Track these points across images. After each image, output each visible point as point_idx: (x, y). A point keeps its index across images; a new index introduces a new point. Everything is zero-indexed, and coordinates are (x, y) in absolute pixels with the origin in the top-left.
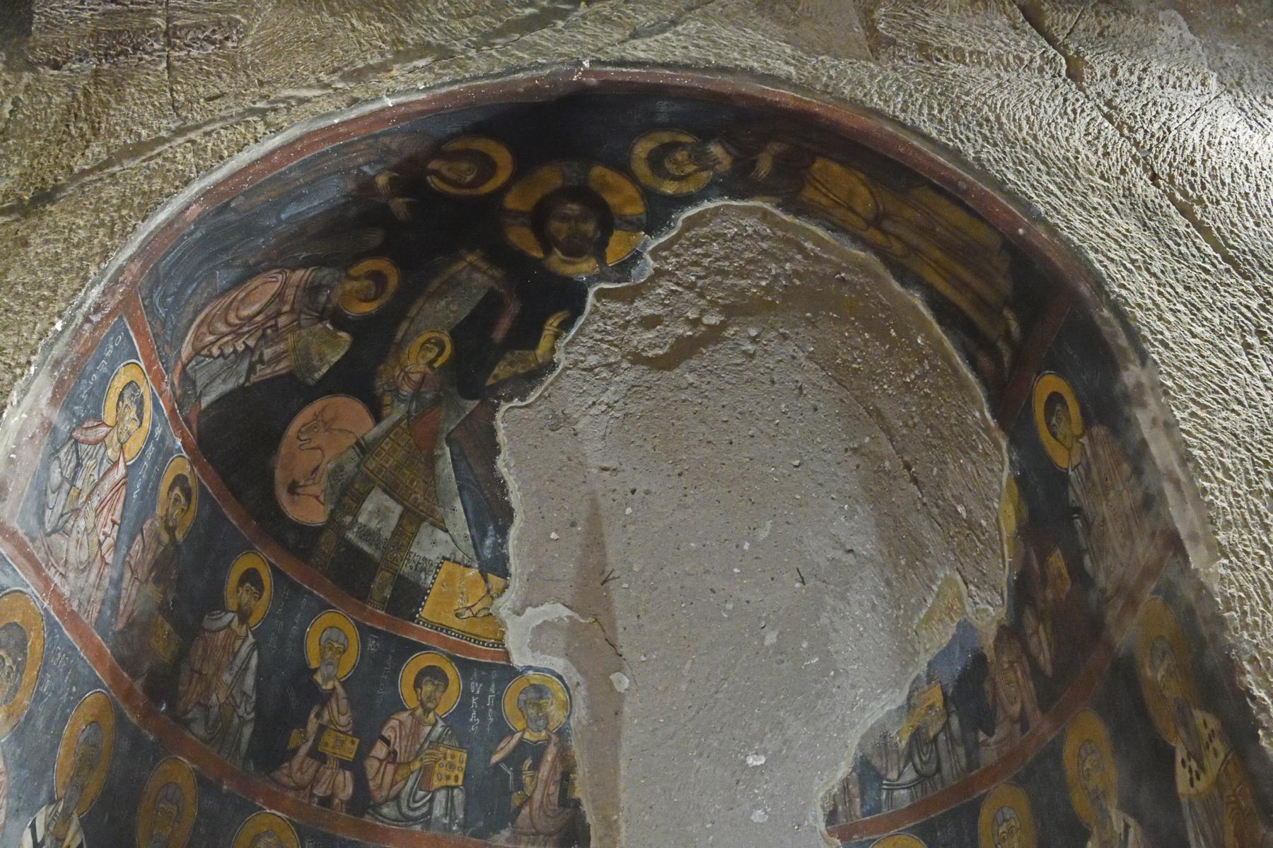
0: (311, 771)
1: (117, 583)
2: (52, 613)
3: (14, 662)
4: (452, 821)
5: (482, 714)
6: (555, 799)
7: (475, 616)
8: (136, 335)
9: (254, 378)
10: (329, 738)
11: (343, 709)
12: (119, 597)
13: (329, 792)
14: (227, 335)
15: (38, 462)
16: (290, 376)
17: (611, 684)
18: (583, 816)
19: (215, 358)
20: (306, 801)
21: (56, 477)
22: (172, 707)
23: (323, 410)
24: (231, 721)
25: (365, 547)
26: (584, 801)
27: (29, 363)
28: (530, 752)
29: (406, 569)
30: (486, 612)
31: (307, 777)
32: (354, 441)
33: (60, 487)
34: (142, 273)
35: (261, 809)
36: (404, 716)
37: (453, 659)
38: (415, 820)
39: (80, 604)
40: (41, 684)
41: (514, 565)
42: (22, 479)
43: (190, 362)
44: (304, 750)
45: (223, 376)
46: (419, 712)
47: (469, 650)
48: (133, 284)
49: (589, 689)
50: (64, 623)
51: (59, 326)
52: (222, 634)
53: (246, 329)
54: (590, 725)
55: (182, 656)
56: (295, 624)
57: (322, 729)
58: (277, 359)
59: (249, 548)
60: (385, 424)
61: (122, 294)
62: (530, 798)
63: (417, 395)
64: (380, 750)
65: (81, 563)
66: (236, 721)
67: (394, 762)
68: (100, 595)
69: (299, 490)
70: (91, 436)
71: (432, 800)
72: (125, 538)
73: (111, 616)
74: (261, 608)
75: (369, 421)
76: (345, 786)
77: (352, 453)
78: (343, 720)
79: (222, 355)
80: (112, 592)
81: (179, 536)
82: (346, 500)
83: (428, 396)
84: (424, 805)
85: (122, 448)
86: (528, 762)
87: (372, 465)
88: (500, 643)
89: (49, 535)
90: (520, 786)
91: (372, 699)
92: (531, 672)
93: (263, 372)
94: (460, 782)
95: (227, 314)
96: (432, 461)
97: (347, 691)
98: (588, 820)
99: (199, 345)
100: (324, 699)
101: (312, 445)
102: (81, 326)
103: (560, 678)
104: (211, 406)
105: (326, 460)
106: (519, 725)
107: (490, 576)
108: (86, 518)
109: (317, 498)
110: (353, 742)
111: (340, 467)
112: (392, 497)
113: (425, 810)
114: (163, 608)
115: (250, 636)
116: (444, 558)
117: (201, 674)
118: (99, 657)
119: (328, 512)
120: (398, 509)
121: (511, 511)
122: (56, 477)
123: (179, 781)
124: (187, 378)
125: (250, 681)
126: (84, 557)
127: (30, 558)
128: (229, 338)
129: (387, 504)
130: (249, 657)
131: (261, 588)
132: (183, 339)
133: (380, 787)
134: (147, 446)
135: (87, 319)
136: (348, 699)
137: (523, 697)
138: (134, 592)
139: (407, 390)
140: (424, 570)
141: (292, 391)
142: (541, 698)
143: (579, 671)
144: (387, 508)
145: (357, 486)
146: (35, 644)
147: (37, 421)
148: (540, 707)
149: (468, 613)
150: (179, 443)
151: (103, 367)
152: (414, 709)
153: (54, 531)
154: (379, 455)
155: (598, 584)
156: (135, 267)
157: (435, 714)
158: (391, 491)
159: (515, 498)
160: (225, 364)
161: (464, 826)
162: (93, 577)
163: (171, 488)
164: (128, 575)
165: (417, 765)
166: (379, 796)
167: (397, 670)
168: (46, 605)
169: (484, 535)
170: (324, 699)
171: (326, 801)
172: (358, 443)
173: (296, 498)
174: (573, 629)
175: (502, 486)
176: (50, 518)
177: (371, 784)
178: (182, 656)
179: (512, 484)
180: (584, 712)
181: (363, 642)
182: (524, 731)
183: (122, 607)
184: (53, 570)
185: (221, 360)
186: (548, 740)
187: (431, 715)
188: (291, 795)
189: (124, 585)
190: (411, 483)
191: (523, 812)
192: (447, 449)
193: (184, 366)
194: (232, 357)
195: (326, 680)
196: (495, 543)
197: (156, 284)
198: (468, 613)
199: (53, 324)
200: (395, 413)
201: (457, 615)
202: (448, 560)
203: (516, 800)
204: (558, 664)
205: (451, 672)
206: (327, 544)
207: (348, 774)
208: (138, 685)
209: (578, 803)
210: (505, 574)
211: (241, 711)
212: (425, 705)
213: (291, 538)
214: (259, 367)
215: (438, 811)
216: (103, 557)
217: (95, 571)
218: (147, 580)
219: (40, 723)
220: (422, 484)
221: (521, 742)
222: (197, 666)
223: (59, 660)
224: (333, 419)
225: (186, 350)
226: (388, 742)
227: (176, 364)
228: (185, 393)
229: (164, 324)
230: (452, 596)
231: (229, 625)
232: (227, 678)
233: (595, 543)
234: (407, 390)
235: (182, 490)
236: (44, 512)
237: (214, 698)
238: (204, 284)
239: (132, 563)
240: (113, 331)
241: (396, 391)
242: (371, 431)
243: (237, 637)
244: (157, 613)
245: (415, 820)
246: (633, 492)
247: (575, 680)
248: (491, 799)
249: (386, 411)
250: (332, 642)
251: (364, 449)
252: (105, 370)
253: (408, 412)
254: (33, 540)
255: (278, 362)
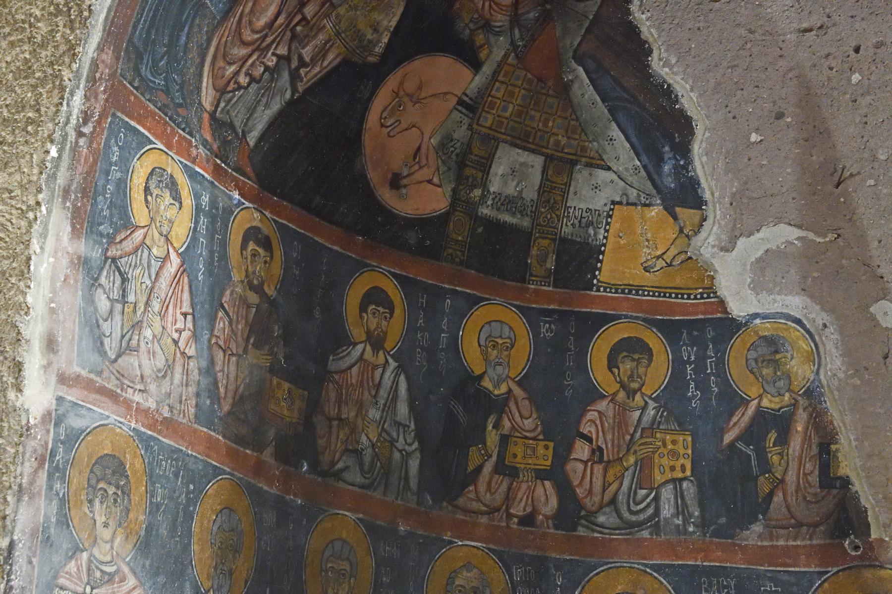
0: (504, 487)
1: (209, 370)
2: (143, 429)
3: (117, 487)
4: (686, 521)
5: (703, 386)
6: (814, 479)
7: (669, 265)
8: (139, 123)
9: (301, 87)
10: (517, 449)
11: (526, 413)
12: (216, 383)
13: (529, 509)
14: (250, 55)
15: (79, 301)
16: (345, 63)
17: (873, 318)
18: (856, 498)
19: (246, 88)
20: (504, 524)
21: (103, 304)
22: (314, 466)
23: (401, 83)
24: (390, 458)
25: (507, 218)
26: (854, 478)
27: (38, 204)
28: (780, 422)
29: (567, 230)
30: (683, 256)
31: (499, 497)
32: (456, 100)
33: (111, 312)
34: (118, 58)
35: (450, 542)
36: (602, 405)
37: (651, 323)
38: (640, 525)
39: (171, 408)
40: (152, 496)
41: (708, 188)
42: (68, 325)
43: (217, 106)
44: (488, 468)
45: (264, 100)
46: (622, 395)
47: (672, 309)
48: (113, 75)
49: (841, 330)
50: (159, 432)
51: (54, 152)
52: (355, 370)
53: (269, 40)
54: (848, 377)
55: (313, 406)
56: (443, 331)
57: (504, 440)
58: (321, 53)
59: (360, 266)
60: (487, 69)
61: (105, 91)
62: (782, 481)
63: (515, 19)
64: (582, 451)
65: (159, 371)
66: (397, 455)
67: (601, 461)
68: (192, 389)
69: (405, 182)
70: (128, 246)
71: (657, 499)
72: (203, 323)
73: (212, 404)
74: (395, 328)
75: (466, 72)
76: (547, 499)
77: (456, 115)
78: (528, 423)
79: (253, 80)
80: (205, 382)
81: (270, 291)
82: (467, 172)
83: (531, 15)
84: (648, 505)
85: (167, 240)
86: (773, 436)
87: (488, 120)
88: (711, 291)
89: (115, 360)
90: (765, 466)
91: (560, 393)
92: (758, 321)
93: (310, 75)
94: (688, 473)
95: (240, 34)
96: (564, 90)
97: (525, 390)
98: (863, 502)
99: (221, 83)
100: (500, 405)
101: (404, 125)
102: (77, 142)
103: (798, 322)
104: (262, 138)
105: (426, 137)
106: (754, 391)
107: (678, 209)
108: (150, 326)
109: (430, 182)
110: (546, 447)
111: (448, 138)
112: (524, 149)
113: (651, 511)
114: (272, 370)
115: (391, 360)
116: (613, 203)
117: (340, 420)
118: (211, 446)
119: (449, 193)
120: (537, 161)
121: (689, 120)
122: (103, 304)
123: (344, 536)
124: (219, 125)
125: (403, 409)
126: (160, 362)
127: (102, 391)
128: (254, 57)
129: (522, 160)
130: (395, 382)
131: (391, 307)
132: (199, 89)
133: (590, 492)
134: (197, 222)
135: (80, 134)
136: (530, 399)
137: (752, 355)
138: (233, 368)
139: (500, 19)
140: (590, 224)
141: (354, 80)
142: (777, 352)
143: (823, 309)
144: (522, 164)
145: (476, 151)
146: (134, 463)
147: (65, 262)
148: (776, 364)
149: (660, 263)
150: (236, 195)
151: (116, 174)
152: (615, 395)
153: (119, 356)
154: (492, 106)
155: (830, 187)
156: (108, 56)
157: (643, 394)
158: (523, 140)
159: (690, 101)
160: (259, 89)
161: (703, 524)
162: (178, 377)
163: (244, 246)
164: (219, 356)
165: (632, 460)
166: (590, 503)
167: (582, 352)
168: (133, 425)
169: (659, 160)
170: (500, 405)
171: (528, 520)
172: (461, 102)
173: (404, 191)
174: (809, 255)
175: (668, 93)
176: (111, 346)
177: (578, 490)
178: (313, 406)
179: (681, 85)
180: (838, 363)
181: (534, 328)
182: (760, 396)
183: (222, 390)
184: (130, 391)
185: (254, 86)
186: (795, 405)
187: (638, 397)
188: (484, 520)
189: (218, 368)
190: (545, 124)
191: (775, 499)
192: (581, 69)
193: (212, 115)
194: (267, 76)
195: (497, 385)
196: (675, 167)
197: (140, 57)
198: (660, 263)
199: (47, 152)
200: (497, 51)
201: (646, 269)
202: (620, 203)
203: (764, 485)
204: (794, 303)
205: (654, 340)
206: (459, 232)
207: (547, 484)
208: (267, 456)
209: (846, 482)
210: (698, 203)
211: (400, 444)
212: (627, 387)
213: (412, 237)
214: (302, 71)
215: (667, 510)
216: (183, 354)
217: (178, 369)
218: (245, 351)
219: (164, 532)
220: (559, 121)
221: (760, 413)
222: (333, 412)
223: (166, 467)
224: (420, 88)
225: (207, 96)
226: (589, 439)
227: (200, 119)
228: (225, 143)
229: (167, 91)
230: (634, 248)
231: (361, 358)
232: (374, 414)
233: (815, 133)
234: (500, 19)
235: (258, 243)
236: (102, 343)
237: (364, 438)
238: (197, 21)
239: (221, 343)
240: (113, 133)
241: (487, 26)
242: (471, 82)
243: (375, 367)
244: (268, 376)
245: (640, 525)
246: (857, 50)
247: (820, 323)
248: (732, 488)
249: (483, 54)
250: (495, 339)
251: (470, 106)
252: (119, 175)
253: (513, 43)
254: (100, 373)
255: (324, 57)
